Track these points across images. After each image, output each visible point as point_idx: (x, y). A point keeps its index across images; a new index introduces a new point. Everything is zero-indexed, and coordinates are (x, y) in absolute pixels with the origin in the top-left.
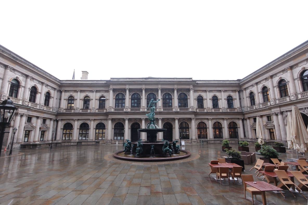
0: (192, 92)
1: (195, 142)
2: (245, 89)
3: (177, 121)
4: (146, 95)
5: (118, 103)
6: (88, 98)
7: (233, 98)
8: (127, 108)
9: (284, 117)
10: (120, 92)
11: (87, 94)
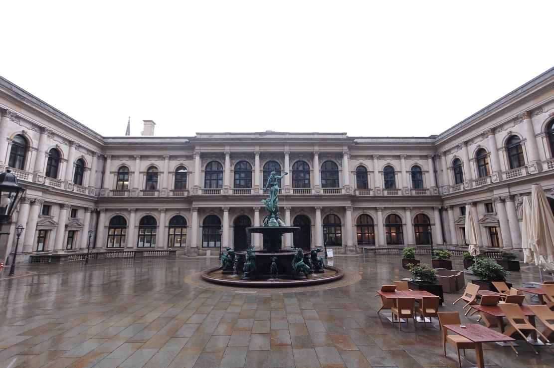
0: (346, 158)
1: (352, 251)
2: (445, 153)
3: (318, 214)
4: (262, 164)
5: (210, 180)
6: (155, 171)
7: (422, 170)
8: (226, 189)
10: (214, 159)
11: (153, 162)
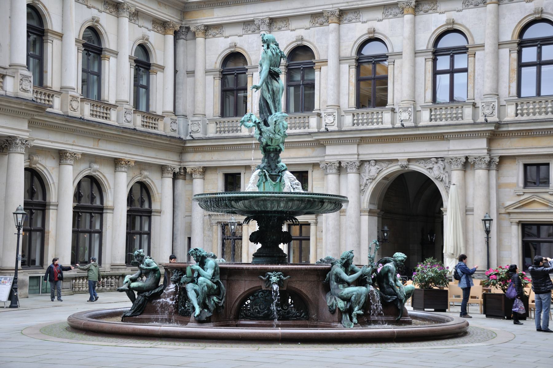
9: (365, 181)
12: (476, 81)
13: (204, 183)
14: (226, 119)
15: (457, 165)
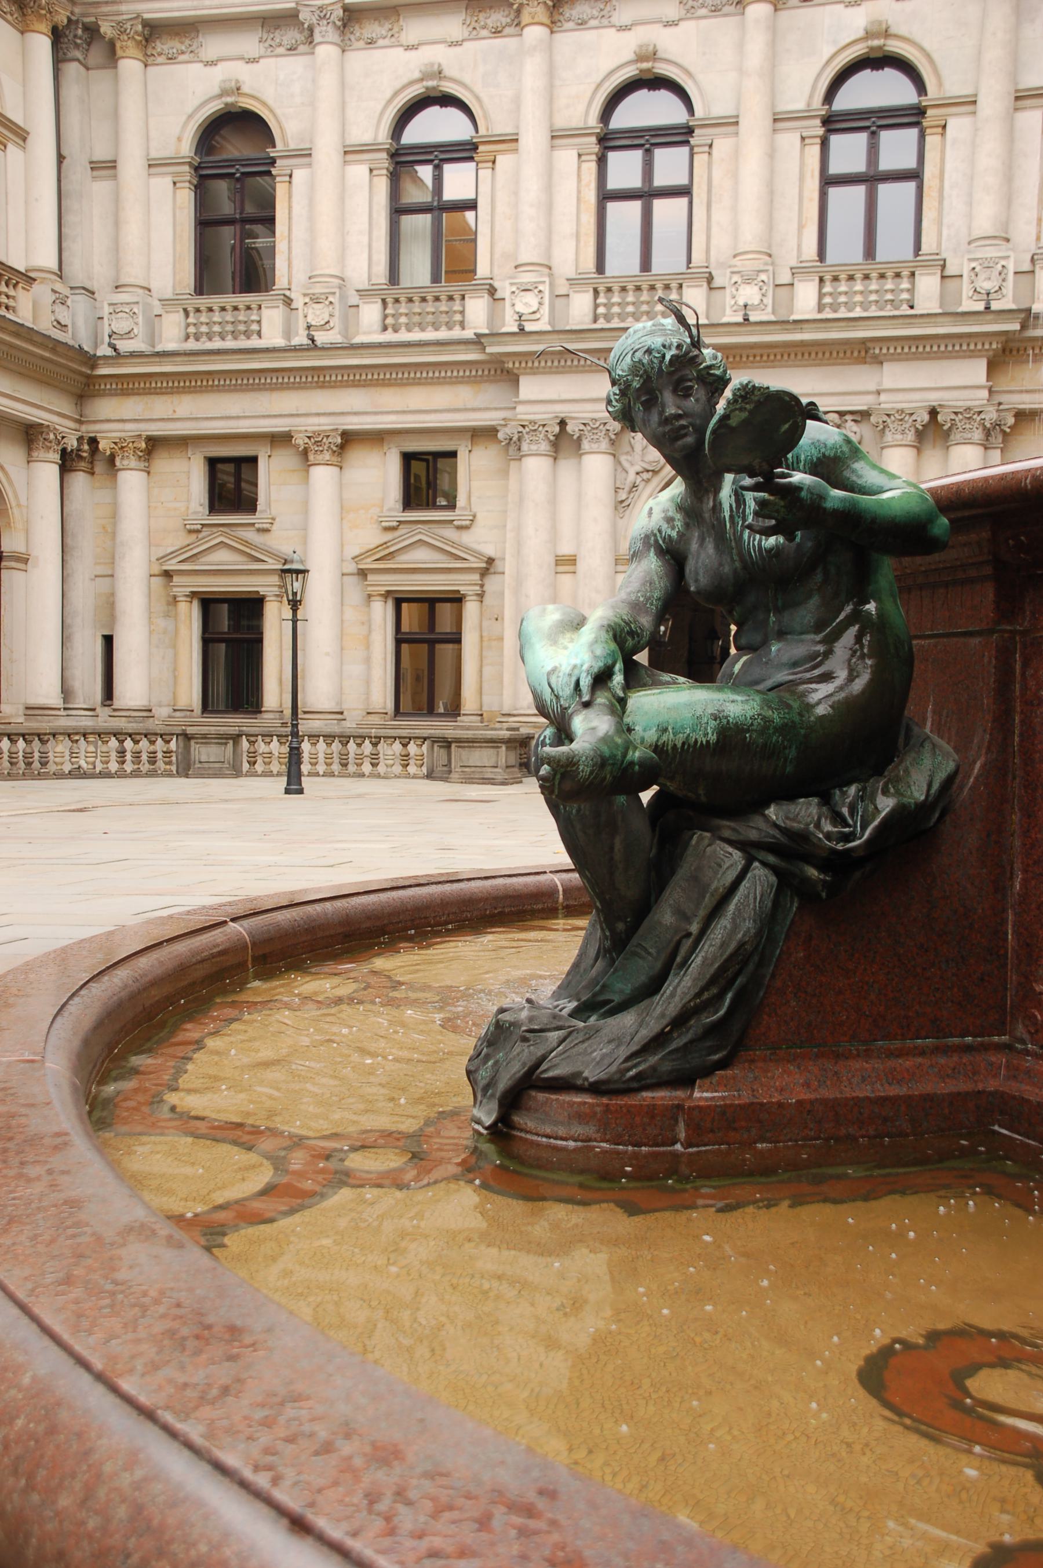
9: (632, 476)
12: (946, 203)
13: (148, 483)
14: (216, 301)
15: (903, 432)
